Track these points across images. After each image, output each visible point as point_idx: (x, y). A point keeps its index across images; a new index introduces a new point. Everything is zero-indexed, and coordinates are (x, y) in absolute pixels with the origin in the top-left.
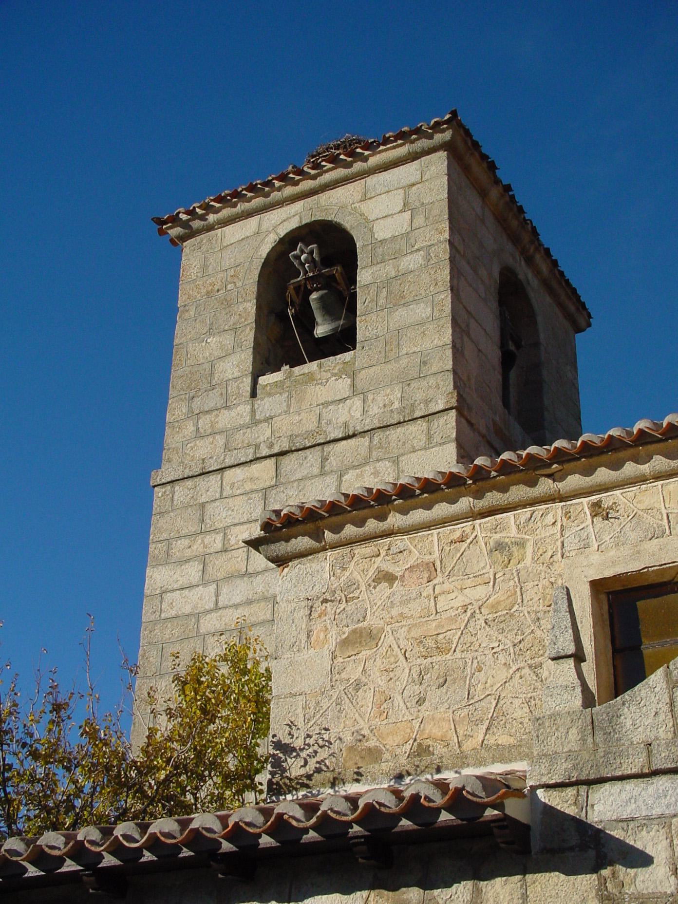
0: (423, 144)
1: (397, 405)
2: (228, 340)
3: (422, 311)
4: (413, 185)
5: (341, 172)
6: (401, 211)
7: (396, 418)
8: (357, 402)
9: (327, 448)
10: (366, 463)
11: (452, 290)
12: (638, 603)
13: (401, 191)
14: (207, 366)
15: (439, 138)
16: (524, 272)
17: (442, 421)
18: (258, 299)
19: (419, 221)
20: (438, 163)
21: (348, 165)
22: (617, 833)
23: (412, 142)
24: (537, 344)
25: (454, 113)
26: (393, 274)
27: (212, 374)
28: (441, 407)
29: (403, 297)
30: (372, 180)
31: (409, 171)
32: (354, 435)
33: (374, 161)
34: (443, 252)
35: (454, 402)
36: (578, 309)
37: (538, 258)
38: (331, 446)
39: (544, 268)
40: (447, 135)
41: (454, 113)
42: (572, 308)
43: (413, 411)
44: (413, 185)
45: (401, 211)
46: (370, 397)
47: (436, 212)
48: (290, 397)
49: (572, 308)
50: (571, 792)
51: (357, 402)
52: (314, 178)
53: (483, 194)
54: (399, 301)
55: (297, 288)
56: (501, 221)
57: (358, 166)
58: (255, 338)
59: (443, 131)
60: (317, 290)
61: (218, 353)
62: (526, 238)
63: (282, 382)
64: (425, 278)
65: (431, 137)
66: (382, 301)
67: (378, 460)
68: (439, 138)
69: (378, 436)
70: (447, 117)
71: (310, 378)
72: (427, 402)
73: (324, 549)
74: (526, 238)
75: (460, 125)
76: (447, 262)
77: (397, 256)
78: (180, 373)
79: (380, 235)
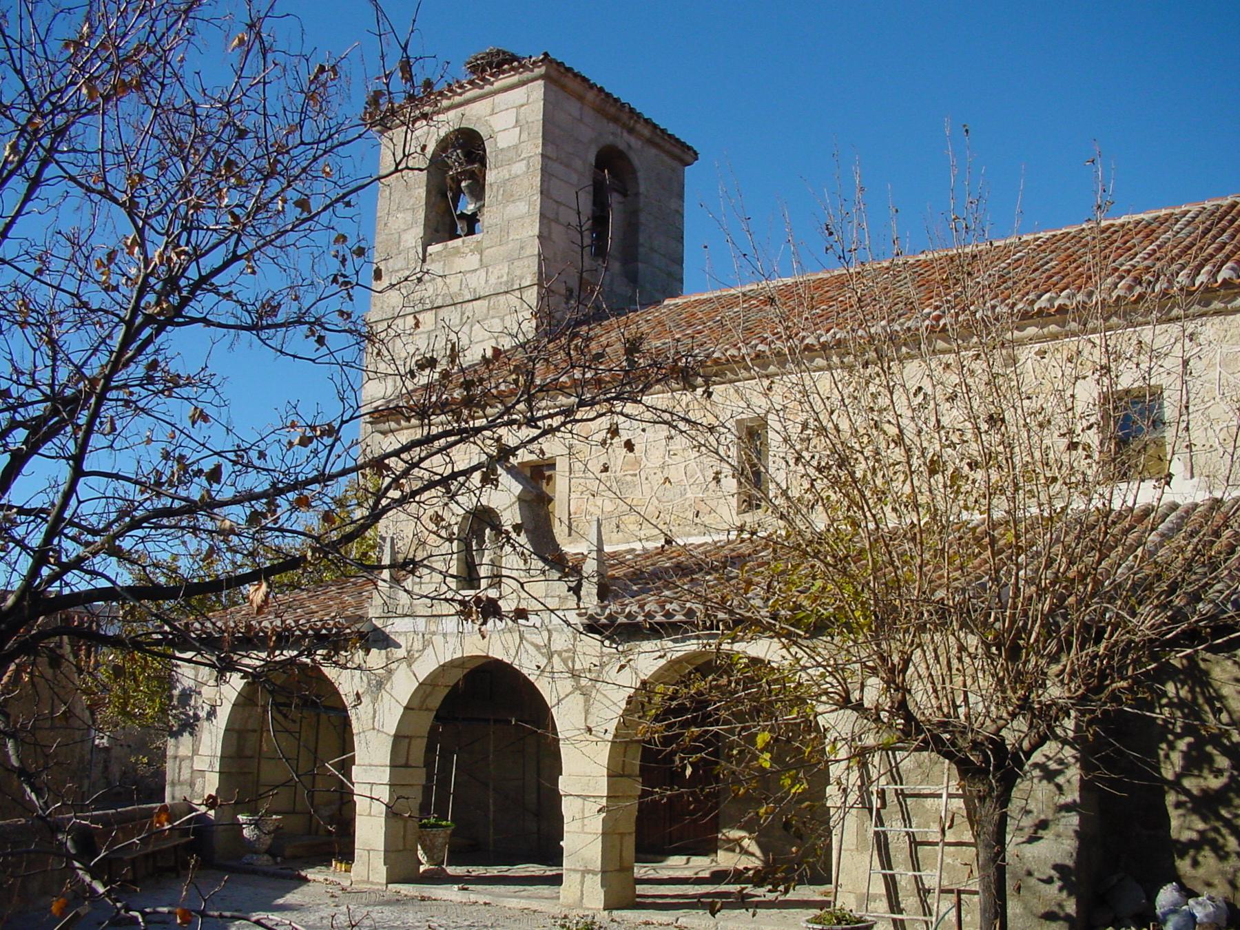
0: (527, 75)
1: (505, 278)
2: (409, 216)
3: (522, 208)
4: (522, 106)
5: (477, 92)
6: (514, 127)
7: (504, 289)
8: (482, 272)
9: (465, 306)
10: (486, 319)
11: (542, 193)
12: (521, 487)
13: (515, 110)
14: (396, 236)
15: (537, 71)
16: (624, 140)
17: (530, 292)
18: (427, 186)
19: (524, 136)
20: (537, 90)
21: (482, 87)
22: (392, 637)
23: (521, 73)
24: (637, 194)
25: (546, 54)
26: (507, 177)
27: (399, 243)
28: (528, 283)
29: (512, 196)
30: (499, 98)
31: (519, 95)
32: (479, 298)
33: (497, 85)
34: (537, 162)
35: (536, 281)
36: (684, 151)
37: (639, 127)
38: (467, 304)
39: (646, 132)
40: (542, 70)
41: (546, 54)
42: (677, 151)
43: (512, 285)
44: (522, 106)
45: (514, 127)
46: (490, 269)
47: (535, 130)
48: (445, 264)
49: (677, 151)
50: (382, 620)
51: (482, 272)
52: (460, 95)
53: (581, 98)
54: (510, 198)
55: (452, 178)
56: (601, 111)
57: (488, 88)
58: (426, 217)
59: (539, 67)
60: (465, 180)
61: (403, 227)
62: (625, 117)
63: (441, 252)
64: (526, 183)
65: (532, 71)
66: (500, 198)
67: (493, 318)
68: (537, 71)
69: (493, 299)
70: (541, 57)
71: (457, 251)
72: (521, 278)
73: (402, 429)
74: (625, 117)
75: (552, 61)
76: (539, 171)
77: (510, 162)
78: (380, 239)
79: (501, 145)
